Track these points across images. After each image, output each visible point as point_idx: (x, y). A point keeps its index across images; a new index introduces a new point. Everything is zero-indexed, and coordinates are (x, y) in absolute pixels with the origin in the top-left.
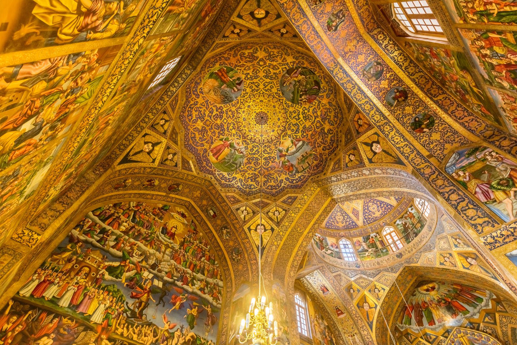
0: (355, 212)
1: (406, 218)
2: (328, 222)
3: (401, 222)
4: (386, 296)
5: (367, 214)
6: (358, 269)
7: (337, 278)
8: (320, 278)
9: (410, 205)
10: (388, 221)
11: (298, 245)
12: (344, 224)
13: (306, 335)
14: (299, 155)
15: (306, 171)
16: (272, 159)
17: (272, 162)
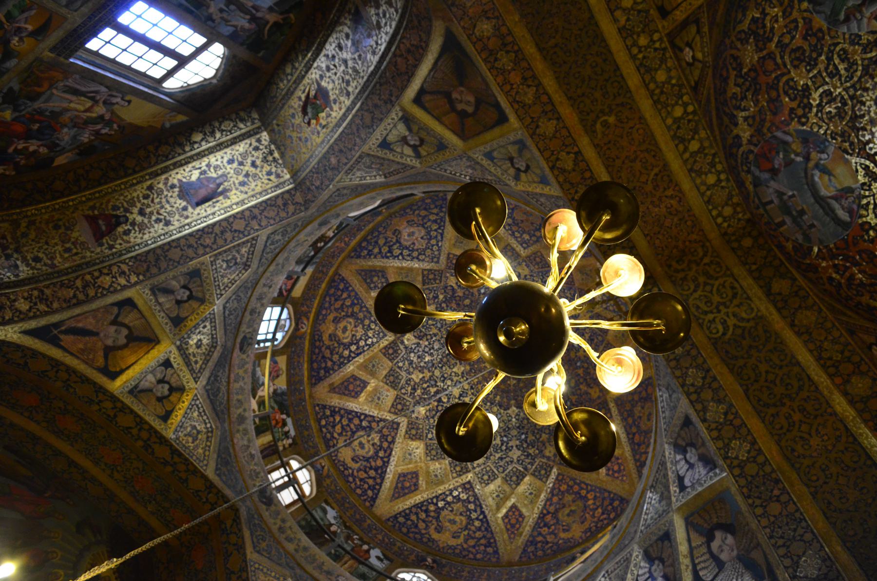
0: (352, 387)
1: (348, 538)
2: (346, 289)
3: (333, 521)
4: (141, 422)
5: (345, 422)
6: (239, 340)
7: (244, 250)
8: (255, 186)
9: (390, 555)
10: (328, 481)
11: (558, 97)
12: (326, 342)
13: (93, 45)
14: (805, 201)
15: (761, 211)
16: (800, 112)
17: (792, 110)
